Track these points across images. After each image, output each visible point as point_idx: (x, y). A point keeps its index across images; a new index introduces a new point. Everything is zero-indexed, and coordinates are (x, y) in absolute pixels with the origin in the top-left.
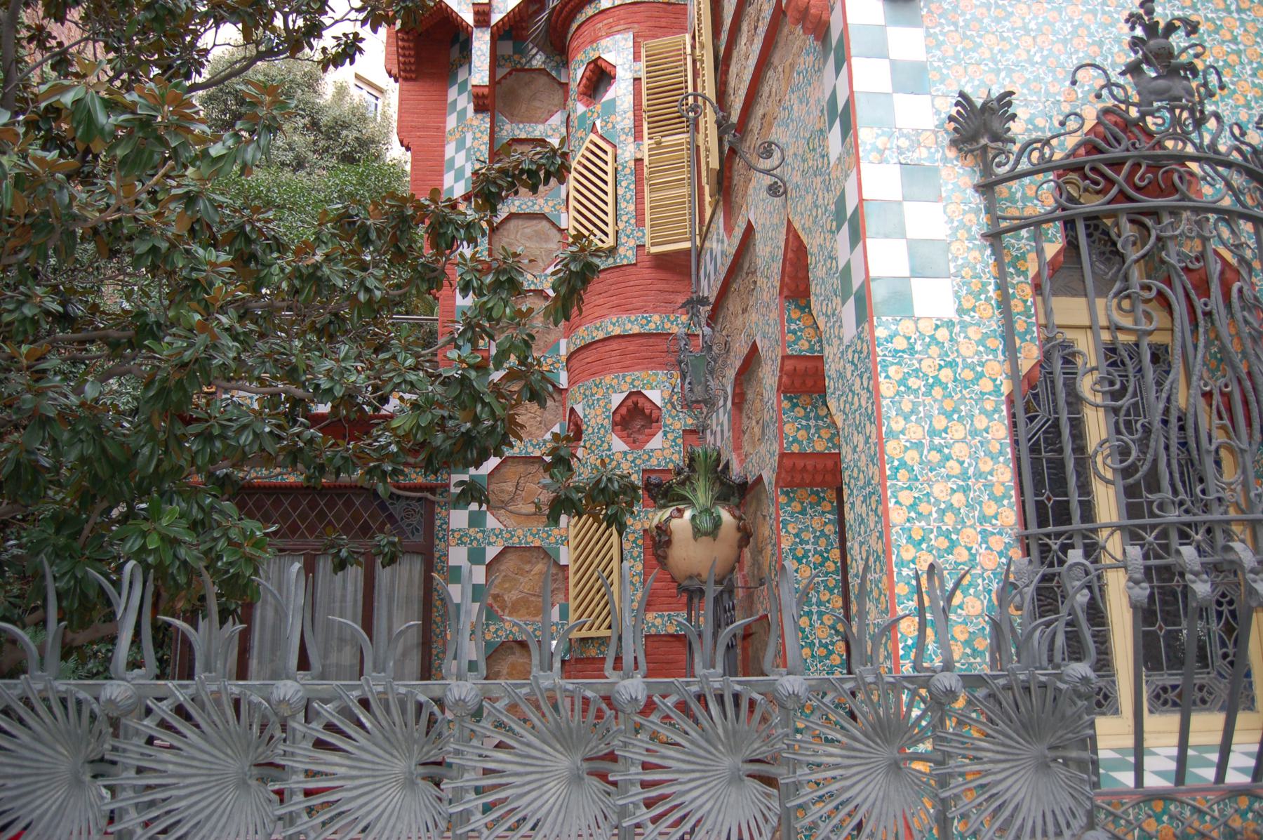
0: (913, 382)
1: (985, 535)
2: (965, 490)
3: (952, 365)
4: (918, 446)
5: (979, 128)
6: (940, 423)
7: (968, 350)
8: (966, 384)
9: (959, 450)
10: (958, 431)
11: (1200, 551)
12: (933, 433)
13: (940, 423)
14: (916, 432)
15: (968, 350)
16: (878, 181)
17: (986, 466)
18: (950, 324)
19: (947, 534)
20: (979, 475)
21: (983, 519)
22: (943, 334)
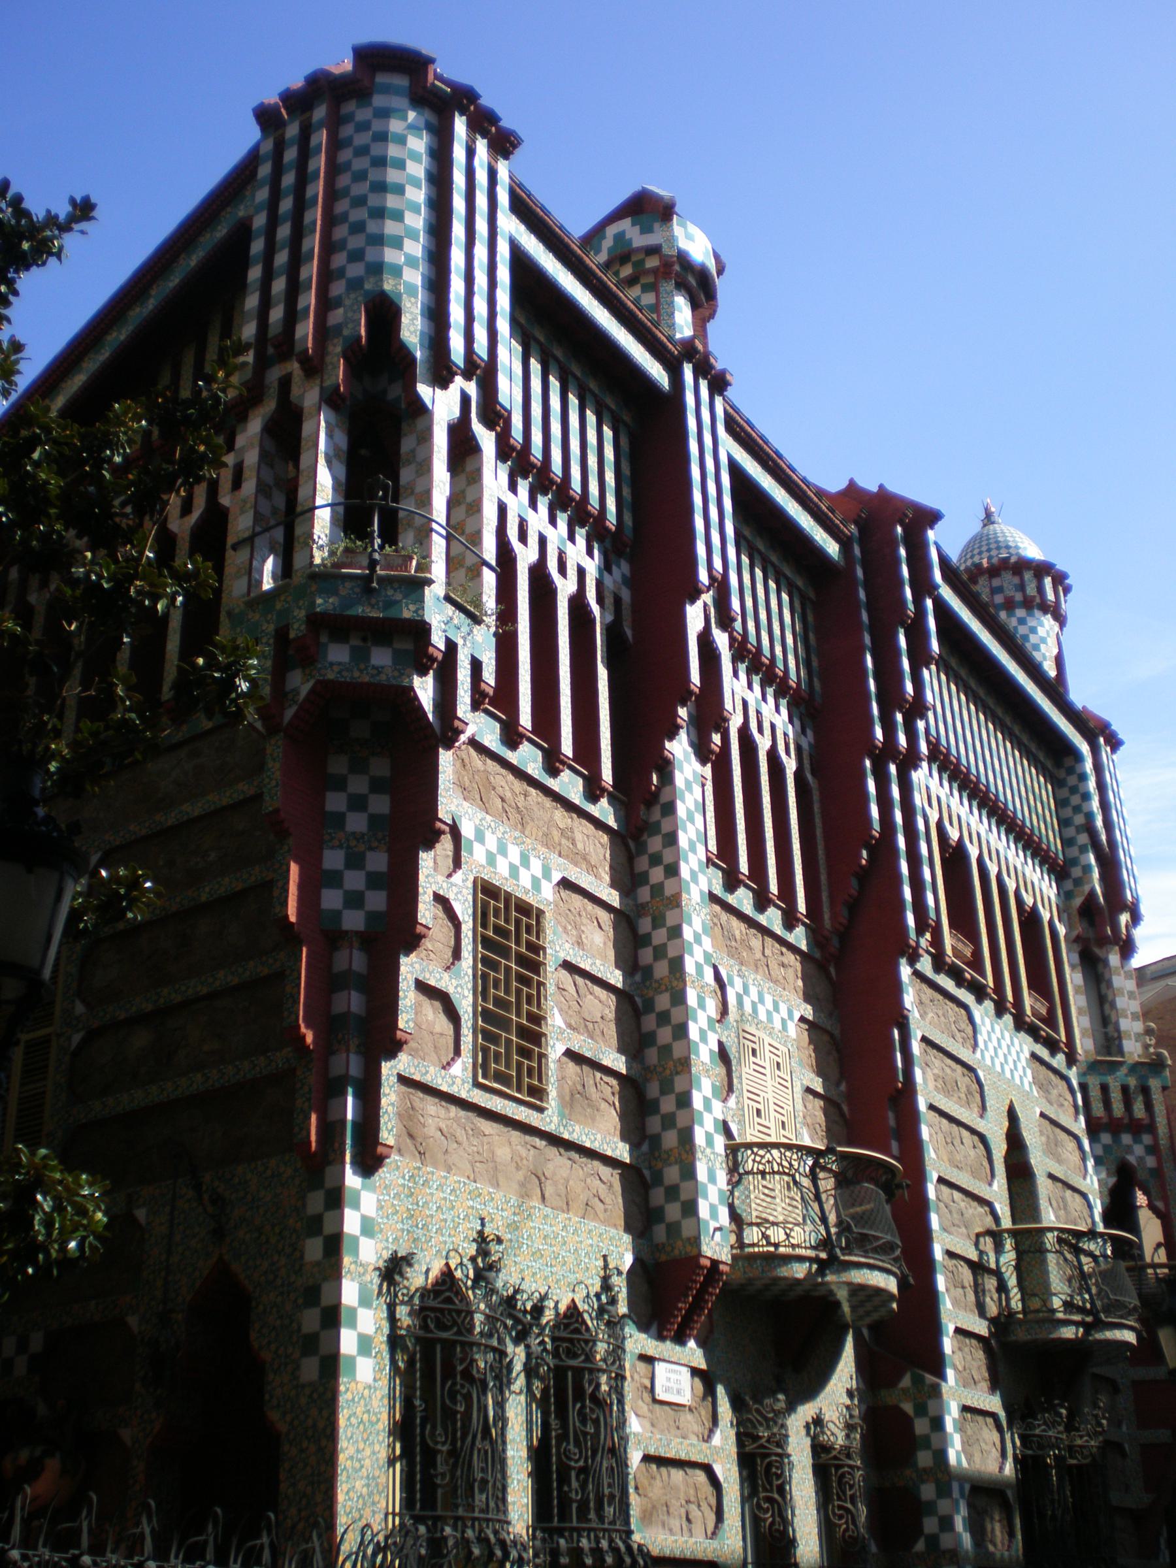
0: (353, 1420)
1: (374, 1512)
2: (368, 1485)
3: (368, 1411)
4: (352, 1458)
5: (393, 1269)
6: (361, 1446)
7: (375, 1403)
8: (372, 1423)
9: (367, 1462)
10: (368, 1452)
11: (428, 1530)
12: (358, 1451)
13: (361, 1446)
14: (351, 1450)
15: (375, 1403)
16: (350, 1293)
17: (377, 1473)
18: (370, 1387)
19: (359, 1510)
20: (374, 1478)
21: (374, 1503)
22: (366, 1392)
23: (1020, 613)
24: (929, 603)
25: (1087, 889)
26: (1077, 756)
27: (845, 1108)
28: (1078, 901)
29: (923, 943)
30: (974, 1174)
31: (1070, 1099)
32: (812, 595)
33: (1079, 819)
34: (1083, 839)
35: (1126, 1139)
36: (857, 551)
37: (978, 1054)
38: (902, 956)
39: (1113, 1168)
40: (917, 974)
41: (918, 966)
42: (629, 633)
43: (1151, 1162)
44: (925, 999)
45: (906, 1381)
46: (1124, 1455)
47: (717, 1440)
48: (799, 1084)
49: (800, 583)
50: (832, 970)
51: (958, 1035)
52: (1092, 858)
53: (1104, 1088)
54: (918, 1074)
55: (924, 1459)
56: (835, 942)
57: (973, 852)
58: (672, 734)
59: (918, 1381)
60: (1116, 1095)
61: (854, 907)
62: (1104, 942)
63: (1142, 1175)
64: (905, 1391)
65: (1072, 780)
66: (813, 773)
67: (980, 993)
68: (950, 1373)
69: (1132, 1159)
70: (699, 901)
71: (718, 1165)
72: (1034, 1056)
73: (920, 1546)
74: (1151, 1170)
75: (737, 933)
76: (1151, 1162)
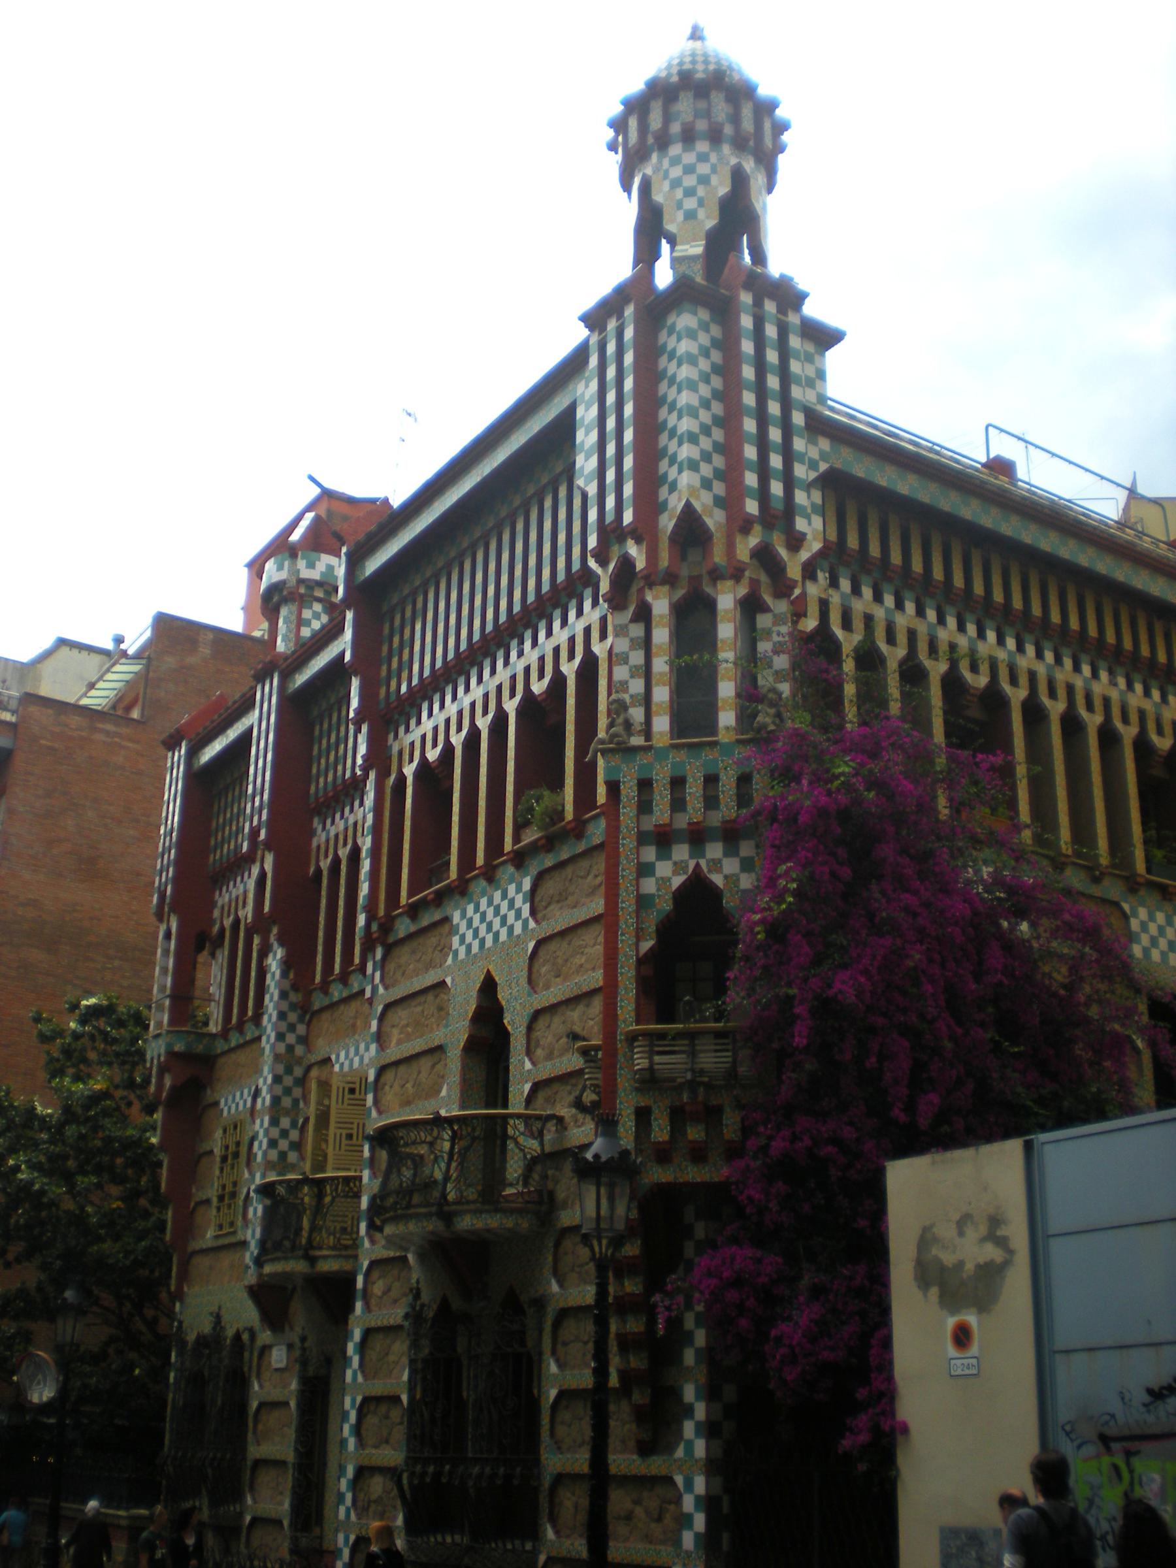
23: (675, 149)
35: (715, 850)
53: (678, 783)
60: (694, 790)
62: (716, 575)
69: (718, 879)
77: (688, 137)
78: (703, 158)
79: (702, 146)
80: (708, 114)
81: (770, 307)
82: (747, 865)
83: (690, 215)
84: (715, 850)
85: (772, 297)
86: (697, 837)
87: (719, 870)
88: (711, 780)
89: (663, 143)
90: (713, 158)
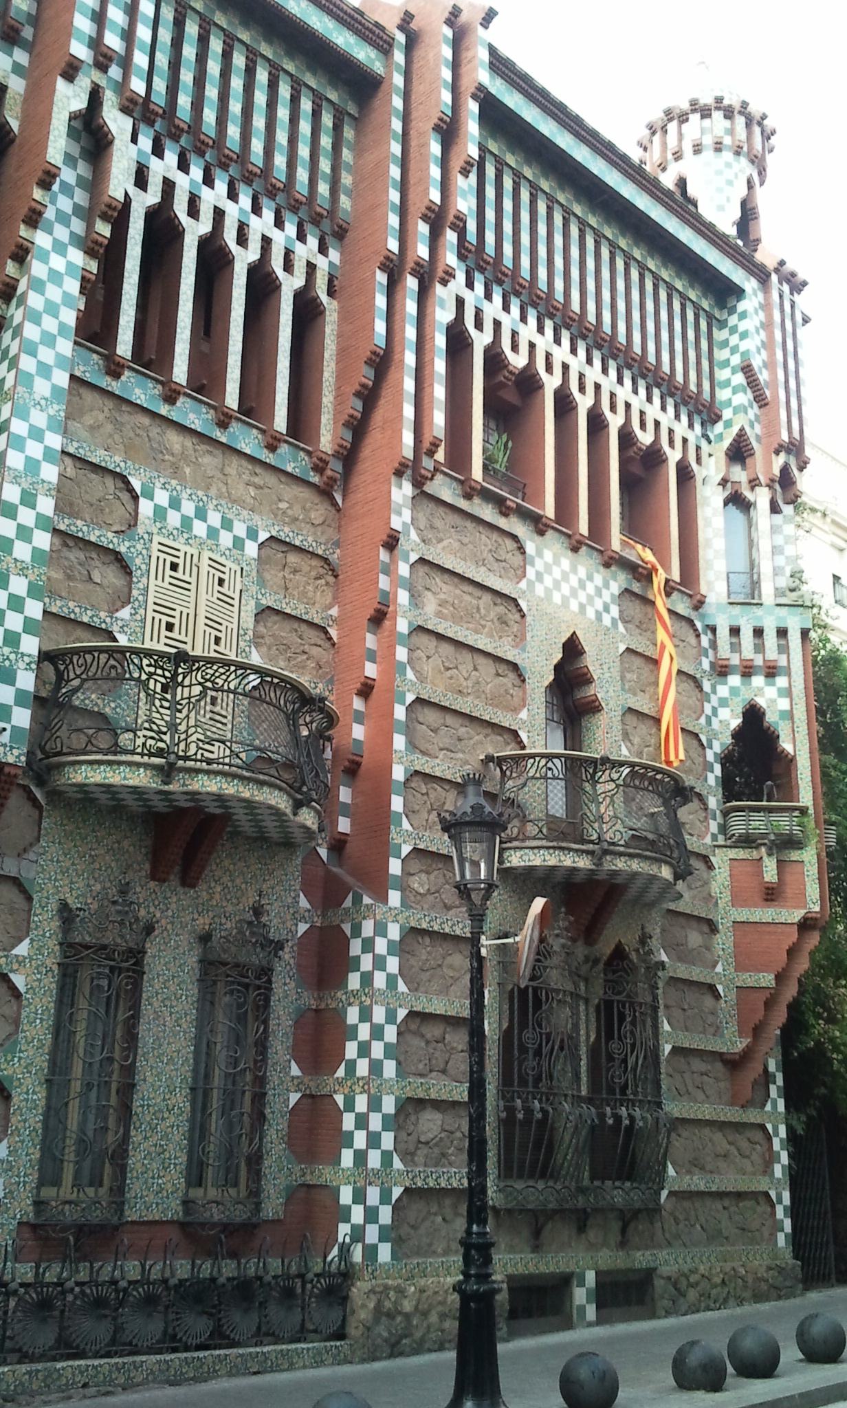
24: (473, 107)
25: (735, 430)
26: (739, 292)
27: (333, 632)
28: (726, 443)
29: (427, 463)
30: (495, 701)
31: (693, 641)
32: (352, 109)
33: (736, 360)
34: (739, 379)
35: (758, 680)
36: (399, 57)
37: (523, 585)
38: (399, 473)
39: (739, 710)
40: (422, 495)
41: (430, 488)
42: (15, 125)
43: (784, 704)
44: (438, 523)
45: (348, 902)
46: (717, 996)
47: (22, 949)
48: (253, 603)
49: (333, 96)
50: (339, 498)
51: (495, 565)
52: (744, 398)
54: (403, 597)
55: (354, 981)
56: (336, 466)
57: (551, 383)
58: (34, 219)
59: (358, 900)
61: (358, 428)
62: (754, 483)
63: (771, 718)
64: (347, 910)
65: (733, 320)
66: (331, 293)
67: (539, 525)
68: (394, 898)
69: (761, 702)
70: (48, 394)
71: (21, 665)
72: (627, 591)
73: (341, 1072)
74: (782, 713)
75: (177, 448)
76: (784, 704)
77: (718, 147)
78: (728, 165)
79: (727, 155)
80: (731, 132)
81: (786, 288)
82: (788, 693)
83: (721, 208)
84: (758, 680)
85: (788, 281)
86: (747, 671)
87: (763, 695)
88: (758, 632)
89: (698, 149)
90: (735, 164)
